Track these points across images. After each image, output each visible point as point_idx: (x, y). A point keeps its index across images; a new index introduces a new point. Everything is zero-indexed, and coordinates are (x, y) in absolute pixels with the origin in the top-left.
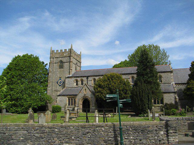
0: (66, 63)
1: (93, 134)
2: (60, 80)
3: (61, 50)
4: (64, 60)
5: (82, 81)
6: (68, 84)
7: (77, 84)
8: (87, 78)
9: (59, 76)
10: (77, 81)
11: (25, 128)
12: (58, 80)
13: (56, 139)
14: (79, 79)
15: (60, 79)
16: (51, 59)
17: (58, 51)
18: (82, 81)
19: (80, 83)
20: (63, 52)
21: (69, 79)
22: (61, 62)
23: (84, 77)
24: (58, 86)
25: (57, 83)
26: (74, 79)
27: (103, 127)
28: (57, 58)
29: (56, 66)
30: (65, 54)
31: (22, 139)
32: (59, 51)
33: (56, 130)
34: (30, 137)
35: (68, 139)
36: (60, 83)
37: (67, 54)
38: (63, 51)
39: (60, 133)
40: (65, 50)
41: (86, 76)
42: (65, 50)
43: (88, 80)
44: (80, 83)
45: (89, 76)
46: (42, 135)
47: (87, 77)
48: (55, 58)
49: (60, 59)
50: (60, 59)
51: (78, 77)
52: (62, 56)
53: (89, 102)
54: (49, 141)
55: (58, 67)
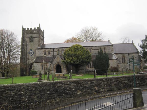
0: (35, 38)
1: (117, 82)
2: (31, 51)
3: (31, 29)
4: (34, 35)
5: (49, 52)
8: (129, 55)
13: (95, 87)
14: (47, 50)
15: (31, 51)
18: (49, 52)
19: (47, 53)
20: (33, 30)
22: (32, 37)
23: (51, 48)
24: (29, 55)
25: (29, 53)
26: (43, 50)
27: (121, 78)
29: (28, 40)
30: (34, 32)
31: (74, 89)
32: (30, 29)
33: (95, 82)
37: (36, 31)
38: (33, 29)
40: (35, 28)
41: (52, 48)
42: (35, 28)
43: (54, 51)
44: (47, 53)
45: (55, 48)
46: (86, 86)
47: (53, 49)
53: (61, 67)
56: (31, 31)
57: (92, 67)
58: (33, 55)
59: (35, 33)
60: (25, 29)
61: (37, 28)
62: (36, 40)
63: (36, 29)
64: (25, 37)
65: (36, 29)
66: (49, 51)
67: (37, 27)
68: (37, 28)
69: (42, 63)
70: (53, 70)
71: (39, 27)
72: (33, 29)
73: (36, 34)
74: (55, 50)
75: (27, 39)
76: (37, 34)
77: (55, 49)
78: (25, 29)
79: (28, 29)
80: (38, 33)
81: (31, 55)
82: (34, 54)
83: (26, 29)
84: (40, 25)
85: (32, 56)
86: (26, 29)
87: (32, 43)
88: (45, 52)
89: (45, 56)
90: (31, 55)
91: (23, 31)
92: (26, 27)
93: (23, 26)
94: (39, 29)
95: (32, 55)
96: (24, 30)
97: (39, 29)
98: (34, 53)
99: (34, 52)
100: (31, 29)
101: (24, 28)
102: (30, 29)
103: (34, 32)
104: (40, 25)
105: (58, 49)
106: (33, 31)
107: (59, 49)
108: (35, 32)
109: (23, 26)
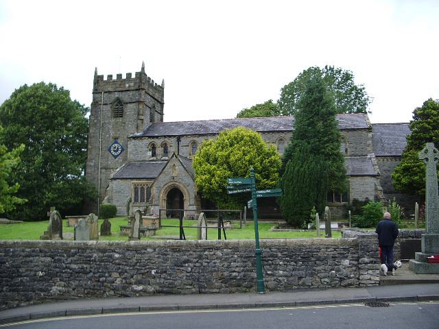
0: (129, 105)
1: (197, 265)
2: (116, 145)
3: (119, 76)
4: (125, 97)
5: (165, 146)
7: (154, 154)
9: (112, 133)
10: (153, 148)
11: (47, 250)
13: (115, 275)
14: (158, 142)
16: (97, 95)
17: (110, 77)
18: (165, 146)
19: (159, 151)
21: (137, 142)
23: (170, 136)
24: (111, 157)
25: (110, 150)
26: (147, 141)
27: (218, 249)
28: (110, 92)
29: (107, 110)
30: (127, 85)
32: (115, 78)
33: (117, 256)
34: (58, 270)
35: (141, 275)
37: (132, 84)
38: (124, 77)
39: (125, 261)
40: (129, 75)
41: (174, 136)
42: (129, 75)
44: (159, 151)
45: (183, 136)
46: (85, 266)
47: (179, 138)
49: (117, 95)
50: (117, 95)
51: (157, 137)
52: (120, 89)
53: (181, 195)
54: (101, 279)
56: (119, 83)
59: (128, 91)
60: (102, 76)
61: (137, 74)
63: (133, 76)
64: (100, 103)
65: (133, 76)
66: (166, 144)
67: (134, 70)
68: (137, 74)
69: (135, 181)
71: (140, 70)
72: (124, 77)
73: (131, 93)
74: (184, 141)
75: (104, 106)
76: (134, 92)
77: (183, 140)
78: (102, 76)
79: (110, 77)
80: (136, 90)
81: (115, 157)
83: (105, 79)
84: (143, 65)
86: (105, 79)
88: (153, 148)
89: (152, 158)
90: (115, 157)
91: (95, 84)
92: (104, 73)
94: (141, 75)
95: (118, 156)
96: (98, 79)
97: (141, 75)
98: (122, 150)
100: (119, 76)
102: (115, 78)
104: (143, 65)
105: (192, 139)
107: (196, 139)
108: (129, 87)
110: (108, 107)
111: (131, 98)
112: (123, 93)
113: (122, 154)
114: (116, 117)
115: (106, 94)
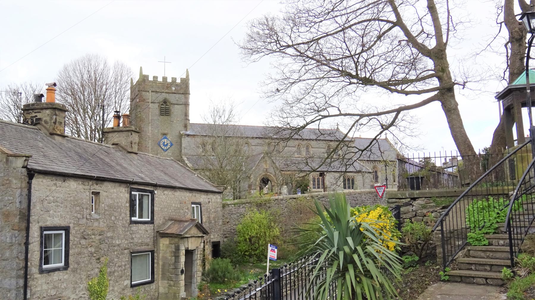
0: (176, 106)
2: (165, 140)
3: (165, 79)
4: (172, 98)
6: (188, 148)
10: (204, 145)
12: (160, 139)
15: (166, 138)
19: (209, 147)
22: (165, 102)
30: (174, 88)
32: (160, 79)
36: (164, 145)
40: (174, 80)
42: (174, 80)
44: (209, 147)
48: (152, 92)
49: (164, 96)
55: (157, 112)
57: (321, 187)
58: (169, 151)
59: (175, 93)
62: (176, 110)
63: (178, 81)
65: (178, 81)
67: (179, 76)
68: (182, 80)
70: (255, 189)
72: (169, 80)
78: (147, 77)
82: (173, 146)
85: (166, 153)
86: (151, 79)
87: (165, 118)
88: (204, 145)
93: (141, 68)
99: (173, 143)
100: (165, 79)
101: (144, 73)
103: (174, 88)
106: (170, 87)
109: (141, 68)
110: (156, 105)
111: (177, 100)
112: (170, 94)
113: (170, 149)
114: (161, 114)
115: (153, 93)
